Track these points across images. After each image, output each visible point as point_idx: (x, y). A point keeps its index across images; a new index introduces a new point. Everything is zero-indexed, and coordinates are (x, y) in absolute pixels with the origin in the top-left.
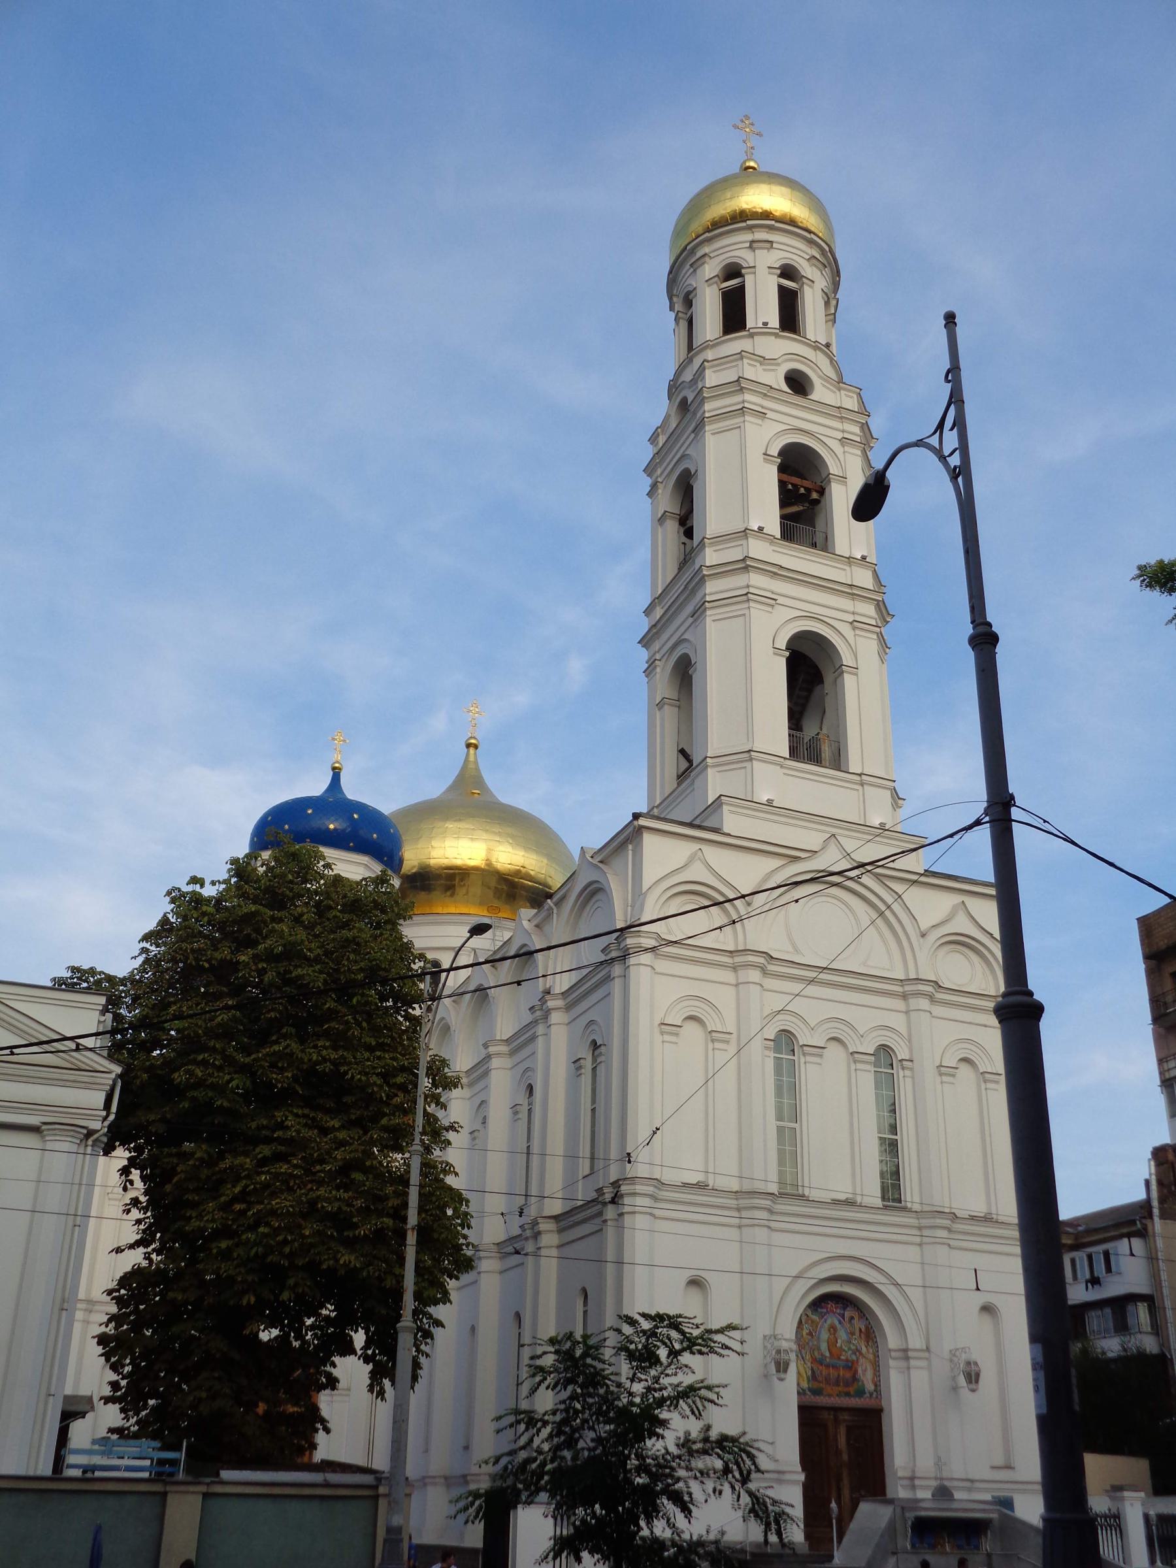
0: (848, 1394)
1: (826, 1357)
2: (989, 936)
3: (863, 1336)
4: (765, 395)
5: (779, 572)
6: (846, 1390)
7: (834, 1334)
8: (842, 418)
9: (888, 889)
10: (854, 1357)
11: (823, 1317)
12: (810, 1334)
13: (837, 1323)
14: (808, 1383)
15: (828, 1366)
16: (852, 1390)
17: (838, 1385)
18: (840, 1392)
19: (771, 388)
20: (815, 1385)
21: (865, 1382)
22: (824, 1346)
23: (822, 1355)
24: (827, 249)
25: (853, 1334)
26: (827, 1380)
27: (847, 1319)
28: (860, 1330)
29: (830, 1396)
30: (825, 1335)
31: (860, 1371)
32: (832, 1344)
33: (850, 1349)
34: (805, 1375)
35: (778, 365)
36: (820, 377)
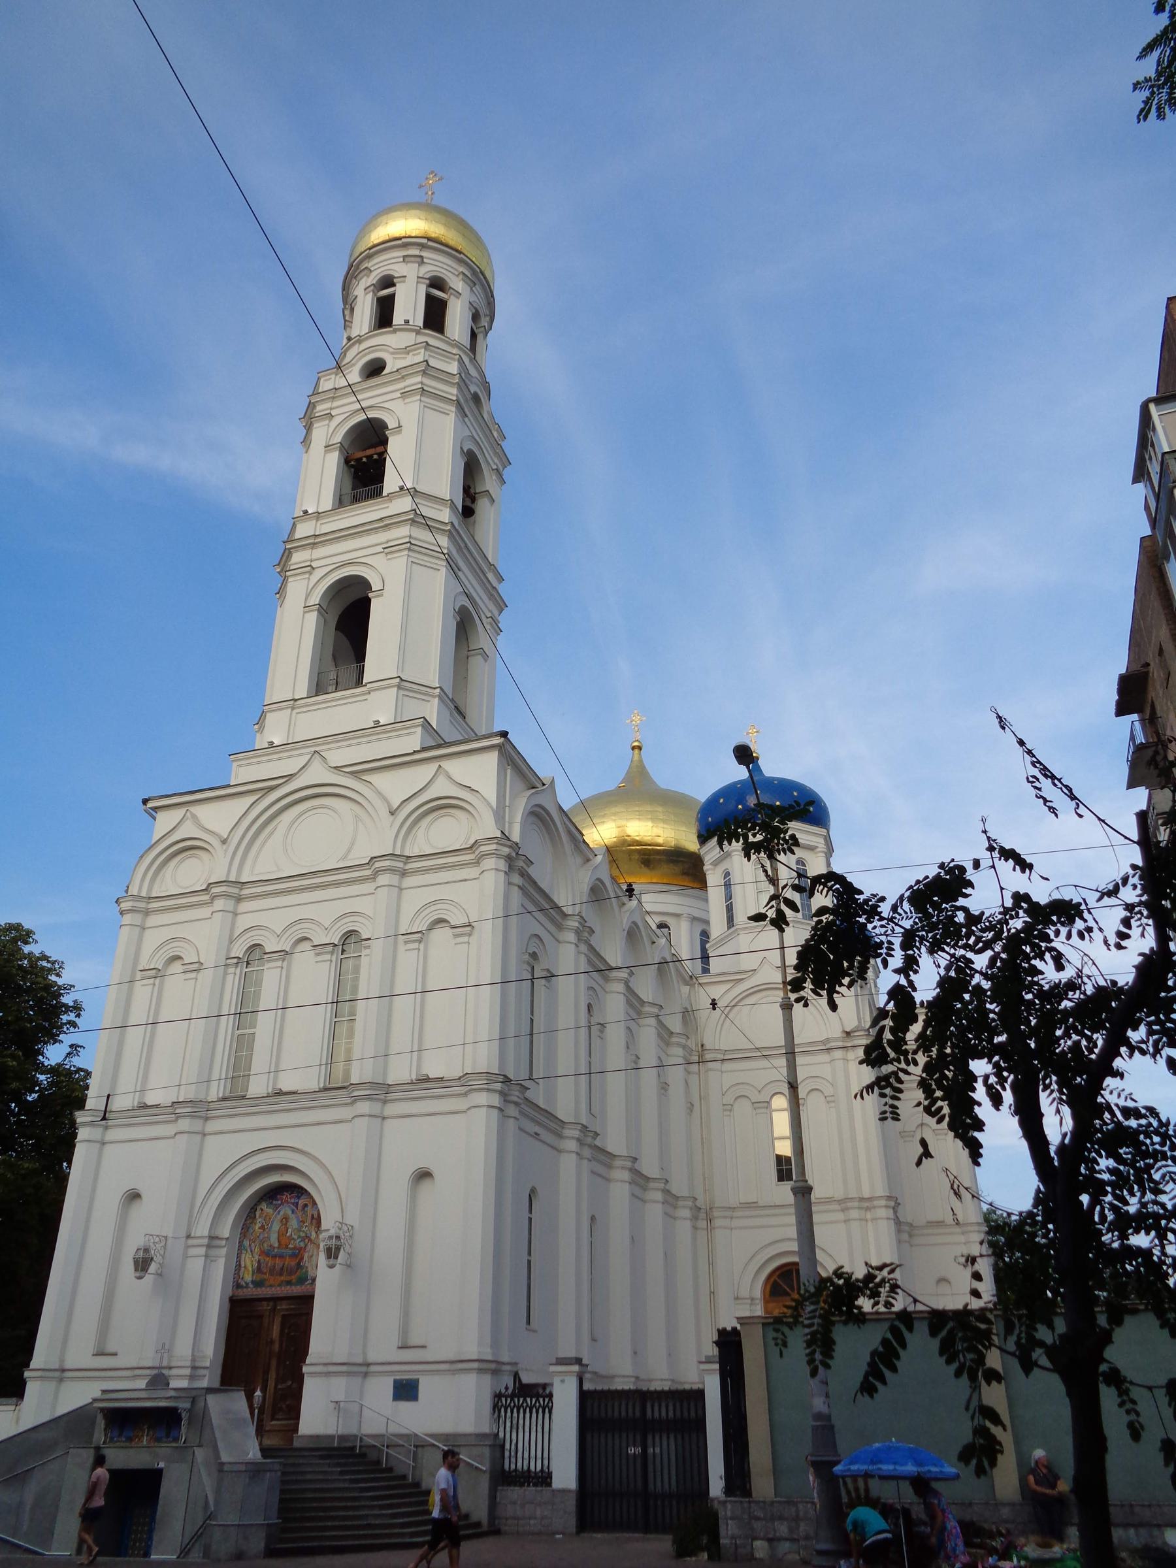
0: (289, 1283)
1: (274, 1248)
2: (468, 789)
3: (314, 1221)
4: (333, 398)
5: (316, 541)
6: (288, 1278)
7: (286, 1224)
8: (403, 377)
9: (364, 782)
10: (302, 1245)
11: (277, 1208)
12: (262, 1227)
13: (290, 1212)
14: (252, 1277)
15: (275, 1257)
16: (294, 1278)
17: (281, 1275)
18: (282, 1282)
19: (336, 389)
20: (258, 1277)
21: (309, 1269)
22: (274, 1240)
23: (271, 1246)
24: (425, 241)
25: (303, 1222)
26: (272, 1271)
27: (300, 1207)
28: (313, 1215)
29: (271, 1286)
30: (276, 1227)
31: (306, 1258)
32: (281, 1235)
33: (299, 1237)
34: (250, 1269)
35: (354, 365)
36: (392, 353)
